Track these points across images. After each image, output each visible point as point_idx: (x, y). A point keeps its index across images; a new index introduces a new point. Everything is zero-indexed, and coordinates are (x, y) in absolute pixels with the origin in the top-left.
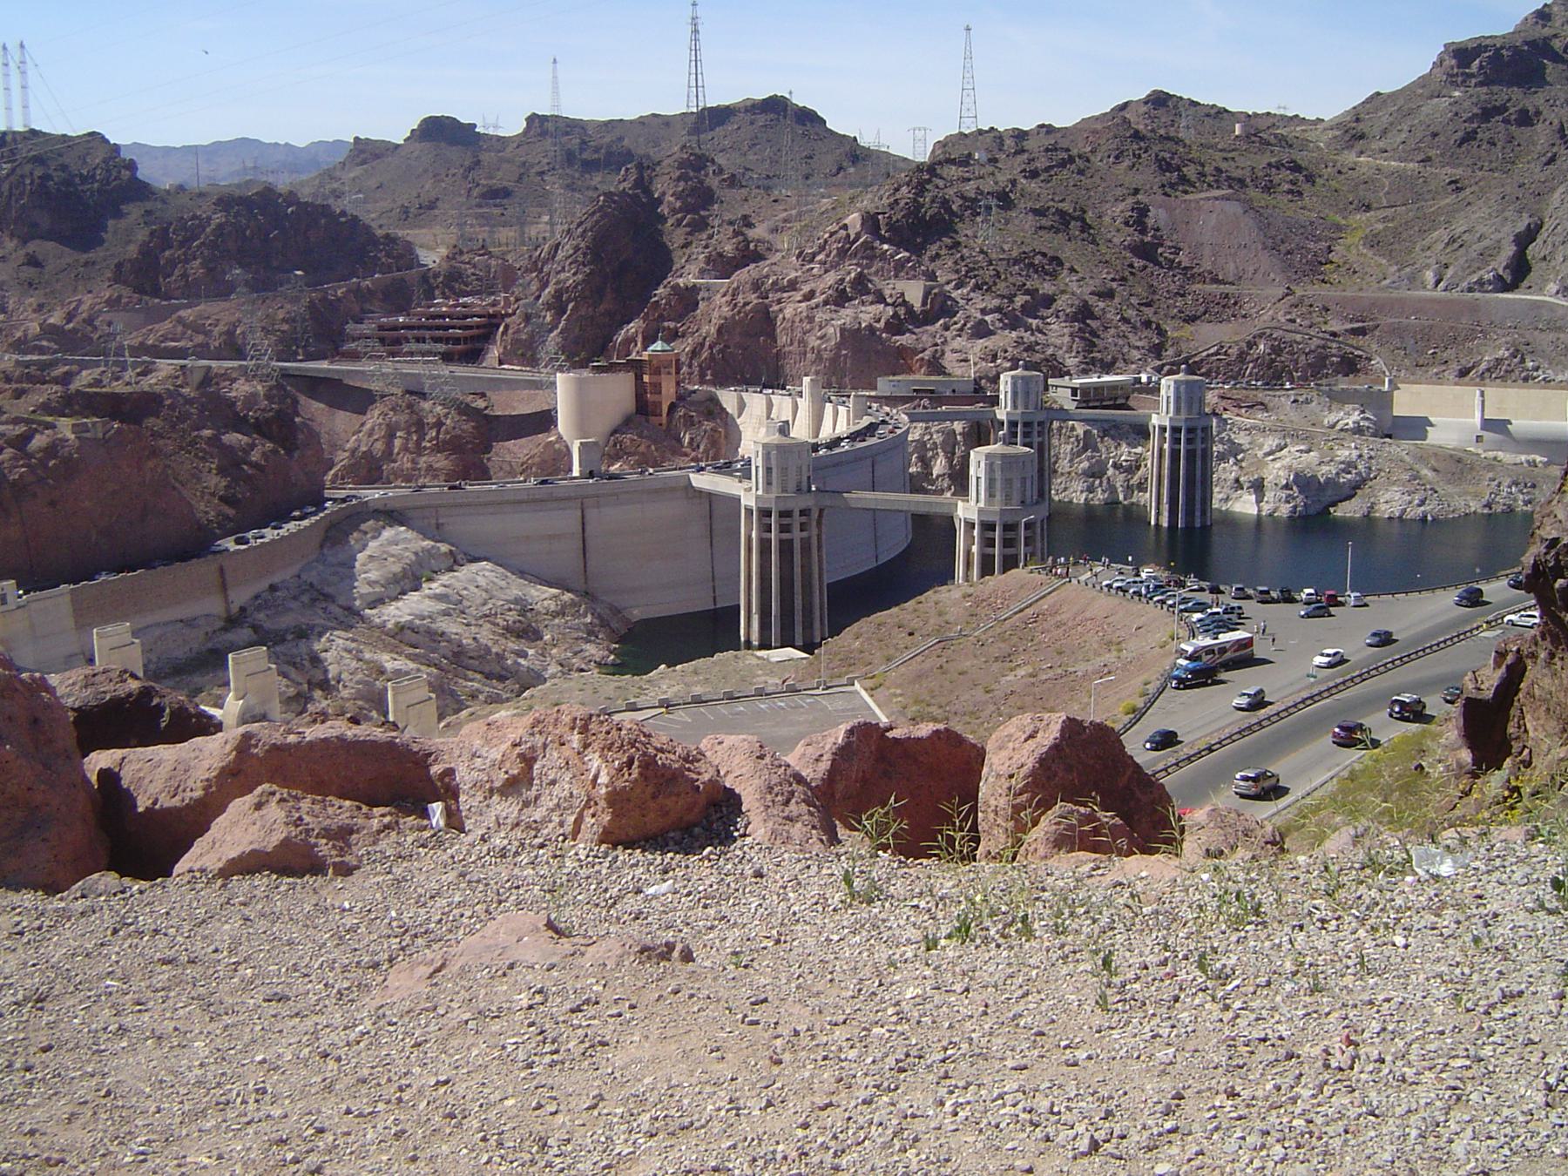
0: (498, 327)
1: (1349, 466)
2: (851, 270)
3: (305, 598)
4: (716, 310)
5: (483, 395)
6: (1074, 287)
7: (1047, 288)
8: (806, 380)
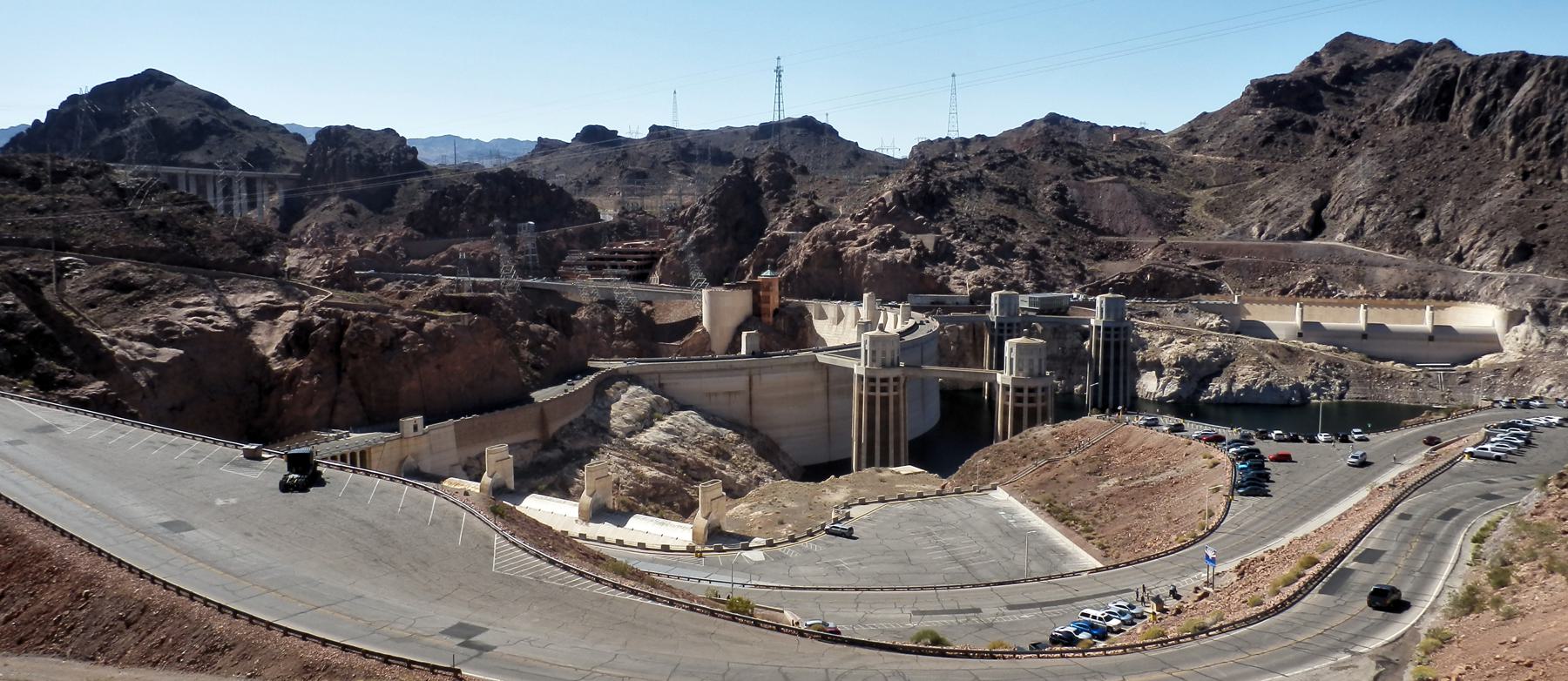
1: (1217, 352)
2: (890, 227)
4: (802, 249)
5: (650, 303)
6: (1025, 238)
7: (1010, 238)
8: (865, 296)
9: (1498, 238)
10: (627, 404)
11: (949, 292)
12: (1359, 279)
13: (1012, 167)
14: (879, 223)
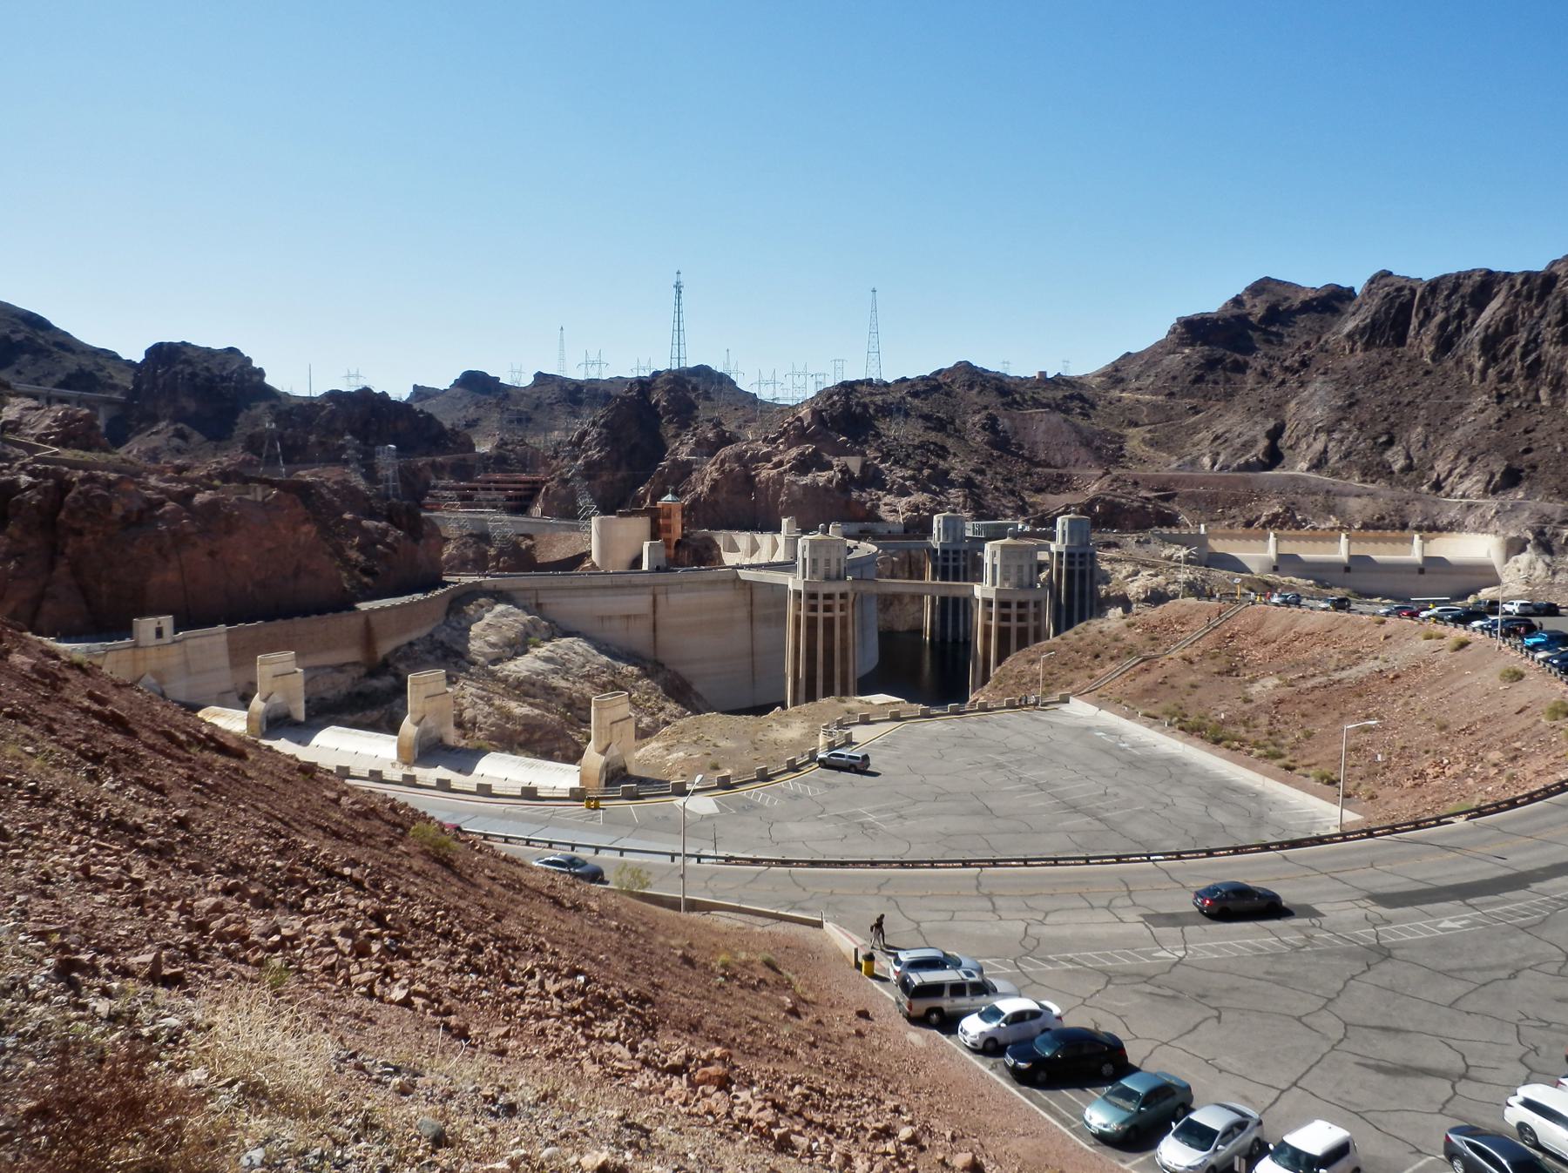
6: (958, 466)
7: (942, 464)
8: (785, 521)
9: (1479, 464)
10: (489, 627)
11: (880, 520)
12: (1330, 510)
13: (936, 395)
14: (797, 444)
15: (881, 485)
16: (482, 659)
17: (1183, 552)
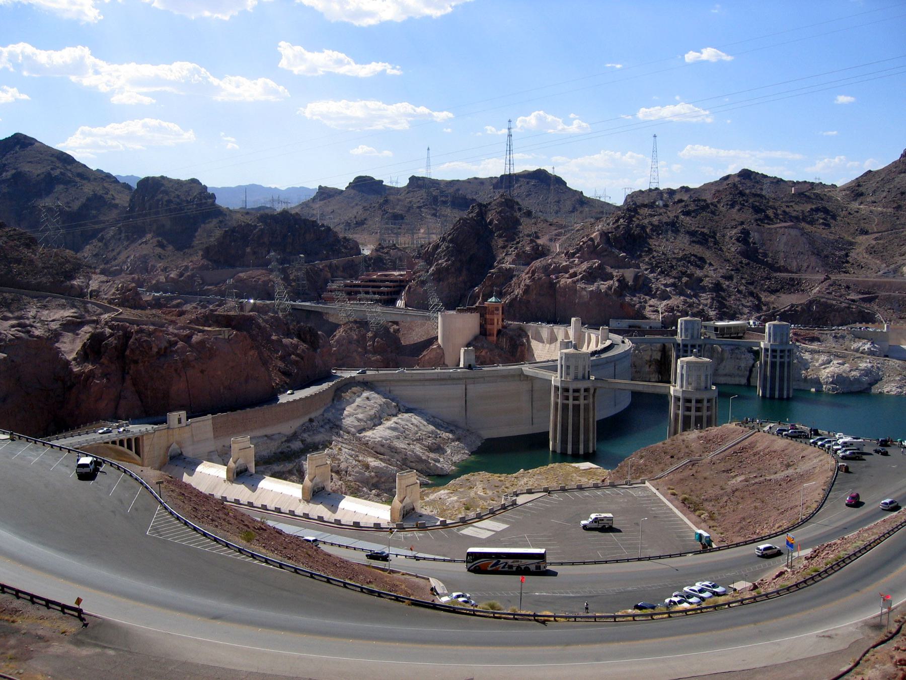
0: (405, 288)
1: (867, 372)
2: (596, 263)
3: (327, 427)
5: (396, 323)
6: (711, 273)
7: (699, 273)
8: (573, 319)
10: (358, 408)
11: (645, 318)
13: (704, 214)
14: (588, 260)
15: (649, 293)
16: (353, 430)
17: (868, 346)
